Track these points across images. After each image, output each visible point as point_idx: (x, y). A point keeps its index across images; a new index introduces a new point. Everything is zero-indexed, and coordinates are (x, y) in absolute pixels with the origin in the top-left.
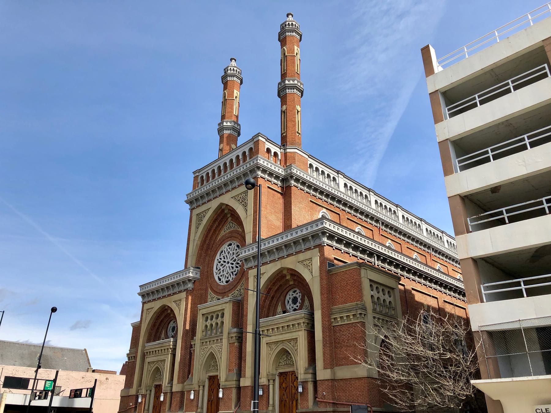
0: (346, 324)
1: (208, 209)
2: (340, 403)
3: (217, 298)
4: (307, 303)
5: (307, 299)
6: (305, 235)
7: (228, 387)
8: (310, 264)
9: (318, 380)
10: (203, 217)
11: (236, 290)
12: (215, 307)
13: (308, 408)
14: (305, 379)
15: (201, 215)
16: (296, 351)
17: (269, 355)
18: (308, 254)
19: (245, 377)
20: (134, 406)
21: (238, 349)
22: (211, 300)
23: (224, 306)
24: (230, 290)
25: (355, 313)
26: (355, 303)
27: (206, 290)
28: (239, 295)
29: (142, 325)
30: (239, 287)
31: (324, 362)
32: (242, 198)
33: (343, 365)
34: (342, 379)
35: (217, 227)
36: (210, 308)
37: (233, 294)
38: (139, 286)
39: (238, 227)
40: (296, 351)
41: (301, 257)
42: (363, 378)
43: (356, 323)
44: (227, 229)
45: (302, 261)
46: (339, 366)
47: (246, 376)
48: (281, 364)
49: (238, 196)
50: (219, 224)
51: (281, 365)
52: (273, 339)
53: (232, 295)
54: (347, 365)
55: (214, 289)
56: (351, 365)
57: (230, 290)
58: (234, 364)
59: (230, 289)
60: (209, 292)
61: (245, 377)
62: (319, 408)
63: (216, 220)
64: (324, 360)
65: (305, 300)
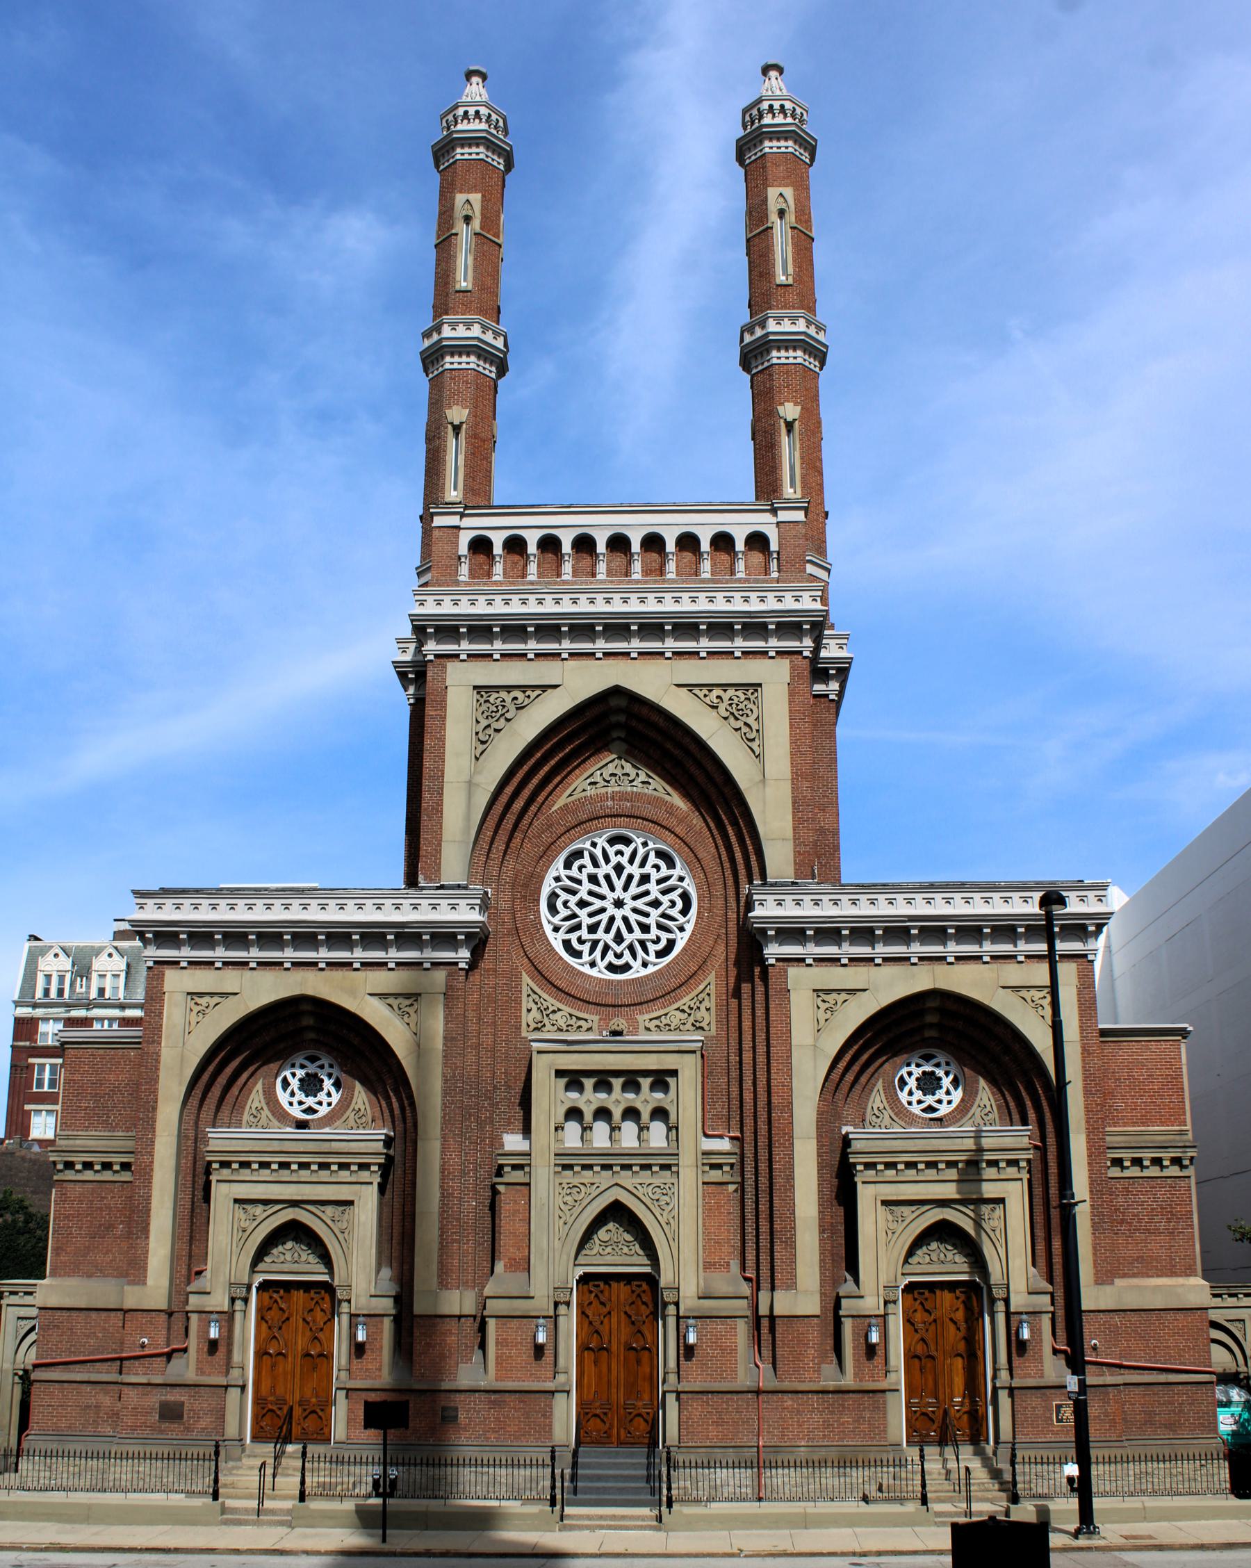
3: (571, 1015)
10: (512, 708)
11: (676, 1006)
15: (495, 695)
19: (792, 1285)
22: (539, 1017)
24: (641, 1004)
27: (515, 976)
28: (689, 1026)
29: (168, 1054)
30: (685, 1002)
31: (1095, 1267)
32: (726, 702)
38: (135, 892)
45: (1016, 989)
46: (1122, 1277)
49: (710, 691)
53: (656, 1022)
55: (562, 985)
57: (641, 1004)
58: (725, 1248)
59: (644, 999)
60: (524, 988)
64: (1095, 1262)
65: (981, 1088)
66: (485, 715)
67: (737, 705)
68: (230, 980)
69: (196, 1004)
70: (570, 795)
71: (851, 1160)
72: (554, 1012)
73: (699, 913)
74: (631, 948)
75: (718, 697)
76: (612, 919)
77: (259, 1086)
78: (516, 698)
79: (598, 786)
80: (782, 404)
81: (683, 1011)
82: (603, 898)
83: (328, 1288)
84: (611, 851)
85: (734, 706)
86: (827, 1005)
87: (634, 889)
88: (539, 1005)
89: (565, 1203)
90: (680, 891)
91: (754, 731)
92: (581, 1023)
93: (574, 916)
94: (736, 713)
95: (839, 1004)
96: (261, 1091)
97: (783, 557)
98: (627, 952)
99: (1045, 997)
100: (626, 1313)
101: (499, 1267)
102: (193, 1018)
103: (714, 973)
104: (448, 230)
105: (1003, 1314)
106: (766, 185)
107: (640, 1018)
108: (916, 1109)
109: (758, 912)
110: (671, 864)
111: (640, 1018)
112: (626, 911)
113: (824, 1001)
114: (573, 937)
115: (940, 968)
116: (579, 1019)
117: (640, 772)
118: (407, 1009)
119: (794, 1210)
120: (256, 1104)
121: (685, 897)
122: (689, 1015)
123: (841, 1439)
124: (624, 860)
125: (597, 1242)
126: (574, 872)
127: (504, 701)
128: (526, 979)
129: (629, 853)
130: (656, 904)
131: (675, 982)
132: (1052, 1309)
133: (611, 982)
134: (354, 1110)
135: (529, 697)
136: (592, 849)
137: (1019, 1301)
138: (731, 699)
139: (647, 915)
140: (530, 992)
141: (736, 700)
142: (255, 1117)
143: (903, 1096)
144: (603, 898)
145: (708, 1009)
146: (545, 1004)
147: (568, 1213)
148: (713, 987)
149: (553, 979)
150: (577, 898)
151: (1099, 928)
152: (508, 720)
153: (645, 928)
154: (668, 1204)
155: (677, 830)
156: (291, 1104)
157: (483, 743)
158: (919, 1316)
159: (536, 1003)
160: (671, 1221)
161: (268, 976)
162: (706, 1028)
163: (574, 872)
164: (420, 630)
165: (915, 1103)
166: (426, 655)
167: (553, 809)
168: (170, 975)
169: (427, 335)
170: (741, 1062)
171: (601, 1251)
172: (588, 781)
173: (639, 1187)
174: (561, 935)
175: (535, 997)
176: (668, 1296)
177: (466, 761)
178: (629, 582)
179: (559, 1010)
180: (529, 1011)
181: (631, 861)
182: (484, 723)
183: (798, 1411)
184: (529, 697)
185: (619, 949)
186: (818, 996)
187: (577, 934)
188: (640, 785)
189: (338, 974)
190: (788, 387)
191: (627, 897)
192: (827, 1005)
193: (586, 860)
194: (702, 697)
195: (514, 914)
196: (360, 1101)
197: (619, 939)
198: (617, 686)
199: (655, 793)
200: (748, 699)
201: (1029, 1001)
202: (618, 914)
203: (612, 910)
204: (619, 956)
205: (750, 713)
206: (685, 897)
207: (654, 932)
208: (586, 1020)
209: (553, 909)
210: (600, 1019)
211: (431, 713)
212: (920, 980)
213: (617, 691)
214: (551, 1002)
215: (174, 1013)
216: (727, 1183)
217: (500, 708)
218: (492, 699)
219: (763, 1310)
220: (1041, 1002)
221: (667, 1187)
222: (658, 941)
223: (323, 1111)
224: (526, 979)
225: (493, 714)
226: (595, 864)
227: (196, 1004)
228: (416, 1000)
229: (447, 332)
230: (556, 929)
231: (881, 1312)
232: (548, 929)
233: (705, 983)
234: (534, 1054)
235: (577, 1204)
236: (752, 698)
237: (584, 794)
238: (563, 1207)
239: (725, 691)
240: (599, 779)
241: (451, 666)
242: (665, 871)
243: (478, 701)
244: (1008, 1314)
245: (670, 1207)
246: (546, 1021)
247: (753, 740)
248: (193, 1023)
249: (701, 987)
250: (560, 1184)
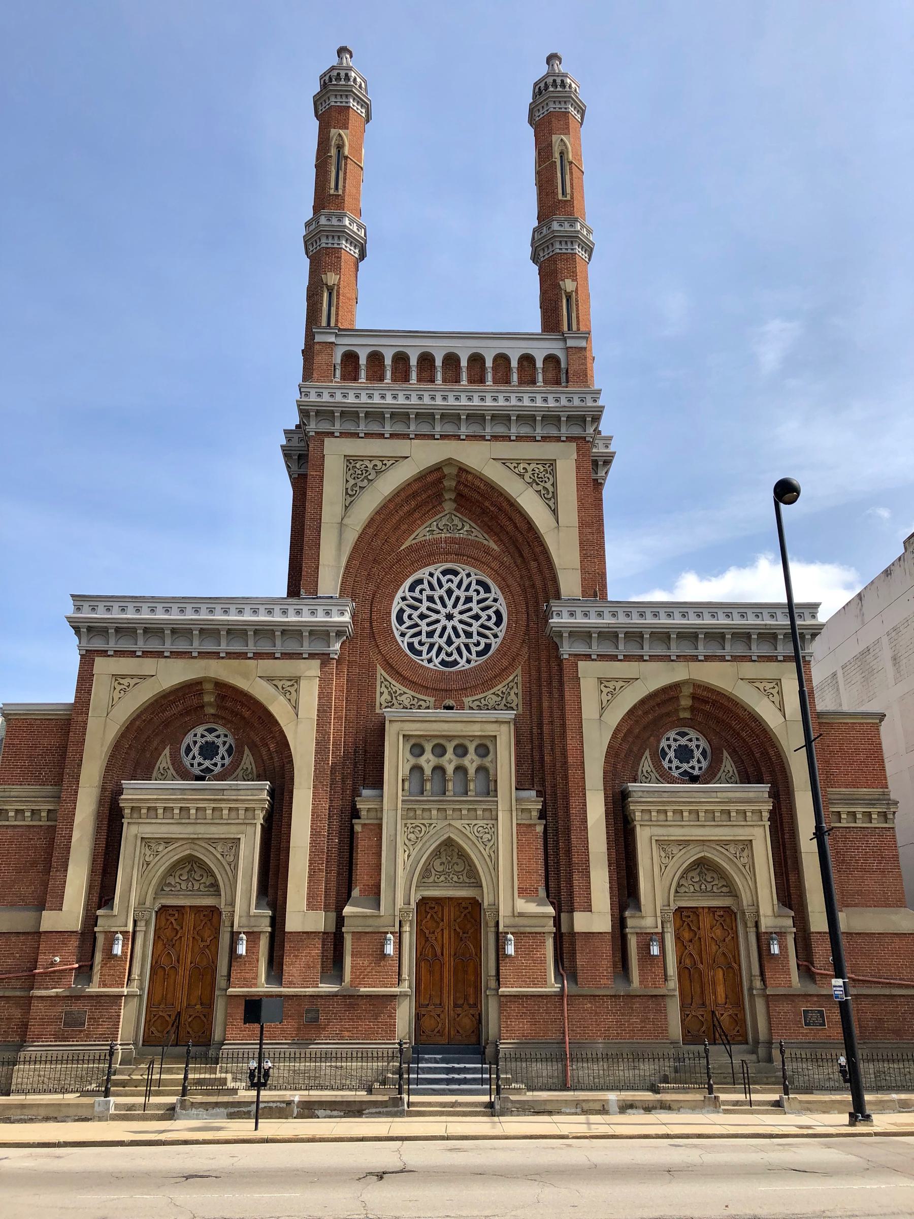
0: (860, 827)
1: (398, 459)
2: (861, 978)
4: (729, 768)
5: (729, 758)
6: (772, 627)
7: (528, 930)
8: (774, 691)
9: (813, 933)
10: (373, 472)
12: (452, 725)
13: (791, 987)
14: (781, 927)
16: (745, 866)
17: (663, 868)
18: (769, 670)
19: (589, 909)
20: (77, 966)
21: (541, 841)
22: (389, 698)
23: (491, 730)
25: (885, 810)
26: (881, 790)
28: (502, 706)
29: (94, 724)
32: (530, 473)
33: (856, 905)
34: (860, 934)
35: (410, 513)
36: (434, 724)
37: (479, 700)
38: (72, 596)
39: (485, 535)
40: (745, 866)
41: (749, 669)
42: (909, 934)
43: (882, 828)
44: (442, 530)
47: (594, 908)
48: (683, 889)
50: (418, 507)
51: (685, 892)
52: (677, 833)
53: (478, 703)
54: (867, 907)
56: (875, 906)
60: (378, 676)
61: (591, 911)
62: (820, 987)
63: (414, 495)
65: (724, 758)
66: (353, 477)
67: (538, 474)
68: (148, 666)
69: (119, 684)
70: (414, 539)
71: (631, 808)
72: (401, 695)
73: (508, 624)
74: (458, 649)
75: (524, 468)
76: (444, 628)
77: (167, 751)
78: (376, 465)
79: (434, 533)
80: (563, 280)
81: (498, 695)
82: (438, 612)
83: (214, 911)
84: (444, 580)
85: (536, 475)
86: (609, 690)
87: (460, 607)
88: (390, 689)
89: (410, 840)
90: (494, 609)
91: (551, 493)
92: (421, 703)
93: (416, 625)
94: (537, 480)
95: (617, 690)
96: (168, 754)
97: (571, 372)
98: (455, 652)
99: (774, 688)
101: (356, 893)
102: (116, 695)
103: (520, 667)
104: (325, 154)
105: (755, 934)
106: (551, 133)
107: (466, 700)
108: (675, 773)
109: (554, 620)
110: (487, 590)
111: (466, 700)
112: (455, 622)
113: (605, 687)
114: (416, 640)
115: (692, 665)
116: (419, 700)
117: (465, 524)
118: (288, 689)
119: (587, 847)
120: (164, 765)
121: (498, 613)
122: (502, 698)
123: (632, 1037)
124: (454, 586)
126: (416, 594)
127: (367, 467)
128: (380, 671)
129: (458, 581)
130: (477, 617)
131: (491, 674)
132: (794, 930)
133: (443, 673)
134: (243, 769)
135: (385, 465)
136: (430, 578)
137: (767, 923)
138: (533, 470)
139: (470, 625)
140: (383, 680)
141: (537, 471)
142: (162, 775)
143: (666, 764)
144: (438, 612)
145: (516, 694)
146: (394, 689)
147: (411, 849)
148: (520, 678)
149: (400, 670)
150: (419, 612)
151: (814, 636)
152: (370, 481)
153: (469, 635)
154: (489, 841)
155: (493, 565)
156: (192, 765)
157: (350, 496)
158: (687, 935)
159: (388, 688)
160: (492, 854)
161: (180, 663)
162: (515, 708)
163: (416, 594)
164: (304, 412)
165: (674, 768)
166: (309, 432)
167: (401, 548)
168: (99, 662)
169: (308, 224)
170: (541, 733)
171: (436, 879)
172: (428, 529)
173: (467, 826)
174: (407, 639)
175: (386, 683)
176: (488, 916)
177: (339, 509)
178: (459, 385)
179: (405, 693)
180: (382, 694)
181: (459, 586)
182: (352, 482)
183: (596, 1013)
184: (385, 465)
185: (449, 650)
186: (602, 683)
187: (419, 638)
188: (465, 533)
189: (234, 663)
190: (567, 269)
191: (455, 612)
192: (609, 690)
193: (426, 585)
194: (513, 469)
195: (371, 623)
196: (248, 762)
197: (449, 642)
198: (450, 459)
199: (476, 539)
200: (546, 471)
201: (762, 690)
202: (449, 625)
203: (444, 622)
204: (449, 655)
205: (547, 480)
206: (498, 613)
207: (476, 638)
208: (425, 701)
209: (400, 621)
210: (435, 700)
211: (312, 473)
212: (678, 673)
213: (449, 462)
214: (398, 687)
215: (100, 692)
217: (364, 472)
218: (358, 466)
219: (564, 929)
220: (771, 691)
222: (478, 644)
223: (217, 770)
224: (380, 671)
225: (359, 476)
226: (432, 588)
227: (119, 684)
228: (296, 682)
229: (323, 221)
230: (403, 635)
231: (659, 930)
232: (397, 634)
233: (514, 675)
234: (387, 723)
236: (549, 470)
237: (424, 538)
239: (529, 464)
240: (435, 528)
241: (327, 441)
242: (483, 595)
243: (347, 466)
244: (758, 935)
245: (492, 843)
246: (394, 701)
247: (550, 499)
248: (116, 699)
249: (511, 678)
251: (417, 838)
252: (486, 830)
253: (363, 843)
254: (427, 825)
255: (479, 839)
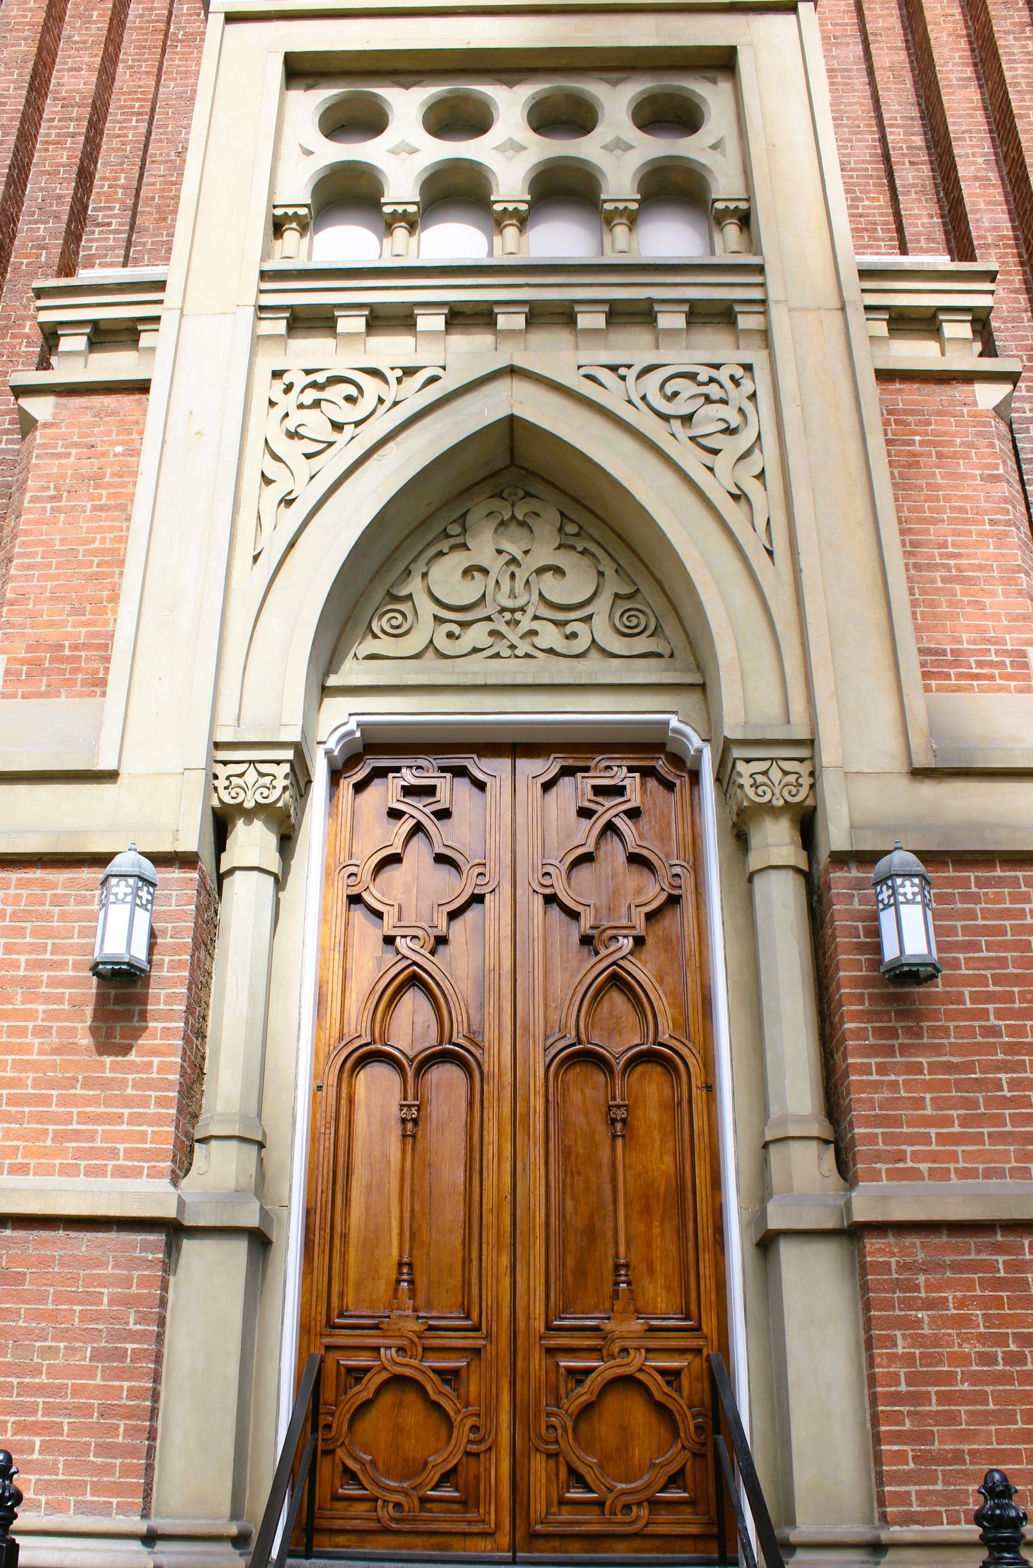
100: (551, 899)
125: (427, 609)
160: (752, 488)
173: (605, 375)
216: (969, 377)
221: (723, 375)
235: (341, 438)
238: (281, 445)
250: (277, 374)
251: (337, 427)
252: (714, 390)
253: (53, 466)
254: (392, 376)
255: (676, 424)
